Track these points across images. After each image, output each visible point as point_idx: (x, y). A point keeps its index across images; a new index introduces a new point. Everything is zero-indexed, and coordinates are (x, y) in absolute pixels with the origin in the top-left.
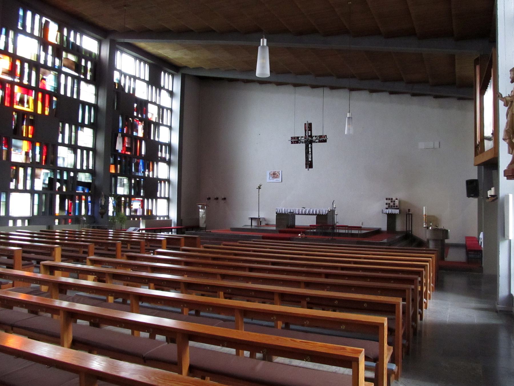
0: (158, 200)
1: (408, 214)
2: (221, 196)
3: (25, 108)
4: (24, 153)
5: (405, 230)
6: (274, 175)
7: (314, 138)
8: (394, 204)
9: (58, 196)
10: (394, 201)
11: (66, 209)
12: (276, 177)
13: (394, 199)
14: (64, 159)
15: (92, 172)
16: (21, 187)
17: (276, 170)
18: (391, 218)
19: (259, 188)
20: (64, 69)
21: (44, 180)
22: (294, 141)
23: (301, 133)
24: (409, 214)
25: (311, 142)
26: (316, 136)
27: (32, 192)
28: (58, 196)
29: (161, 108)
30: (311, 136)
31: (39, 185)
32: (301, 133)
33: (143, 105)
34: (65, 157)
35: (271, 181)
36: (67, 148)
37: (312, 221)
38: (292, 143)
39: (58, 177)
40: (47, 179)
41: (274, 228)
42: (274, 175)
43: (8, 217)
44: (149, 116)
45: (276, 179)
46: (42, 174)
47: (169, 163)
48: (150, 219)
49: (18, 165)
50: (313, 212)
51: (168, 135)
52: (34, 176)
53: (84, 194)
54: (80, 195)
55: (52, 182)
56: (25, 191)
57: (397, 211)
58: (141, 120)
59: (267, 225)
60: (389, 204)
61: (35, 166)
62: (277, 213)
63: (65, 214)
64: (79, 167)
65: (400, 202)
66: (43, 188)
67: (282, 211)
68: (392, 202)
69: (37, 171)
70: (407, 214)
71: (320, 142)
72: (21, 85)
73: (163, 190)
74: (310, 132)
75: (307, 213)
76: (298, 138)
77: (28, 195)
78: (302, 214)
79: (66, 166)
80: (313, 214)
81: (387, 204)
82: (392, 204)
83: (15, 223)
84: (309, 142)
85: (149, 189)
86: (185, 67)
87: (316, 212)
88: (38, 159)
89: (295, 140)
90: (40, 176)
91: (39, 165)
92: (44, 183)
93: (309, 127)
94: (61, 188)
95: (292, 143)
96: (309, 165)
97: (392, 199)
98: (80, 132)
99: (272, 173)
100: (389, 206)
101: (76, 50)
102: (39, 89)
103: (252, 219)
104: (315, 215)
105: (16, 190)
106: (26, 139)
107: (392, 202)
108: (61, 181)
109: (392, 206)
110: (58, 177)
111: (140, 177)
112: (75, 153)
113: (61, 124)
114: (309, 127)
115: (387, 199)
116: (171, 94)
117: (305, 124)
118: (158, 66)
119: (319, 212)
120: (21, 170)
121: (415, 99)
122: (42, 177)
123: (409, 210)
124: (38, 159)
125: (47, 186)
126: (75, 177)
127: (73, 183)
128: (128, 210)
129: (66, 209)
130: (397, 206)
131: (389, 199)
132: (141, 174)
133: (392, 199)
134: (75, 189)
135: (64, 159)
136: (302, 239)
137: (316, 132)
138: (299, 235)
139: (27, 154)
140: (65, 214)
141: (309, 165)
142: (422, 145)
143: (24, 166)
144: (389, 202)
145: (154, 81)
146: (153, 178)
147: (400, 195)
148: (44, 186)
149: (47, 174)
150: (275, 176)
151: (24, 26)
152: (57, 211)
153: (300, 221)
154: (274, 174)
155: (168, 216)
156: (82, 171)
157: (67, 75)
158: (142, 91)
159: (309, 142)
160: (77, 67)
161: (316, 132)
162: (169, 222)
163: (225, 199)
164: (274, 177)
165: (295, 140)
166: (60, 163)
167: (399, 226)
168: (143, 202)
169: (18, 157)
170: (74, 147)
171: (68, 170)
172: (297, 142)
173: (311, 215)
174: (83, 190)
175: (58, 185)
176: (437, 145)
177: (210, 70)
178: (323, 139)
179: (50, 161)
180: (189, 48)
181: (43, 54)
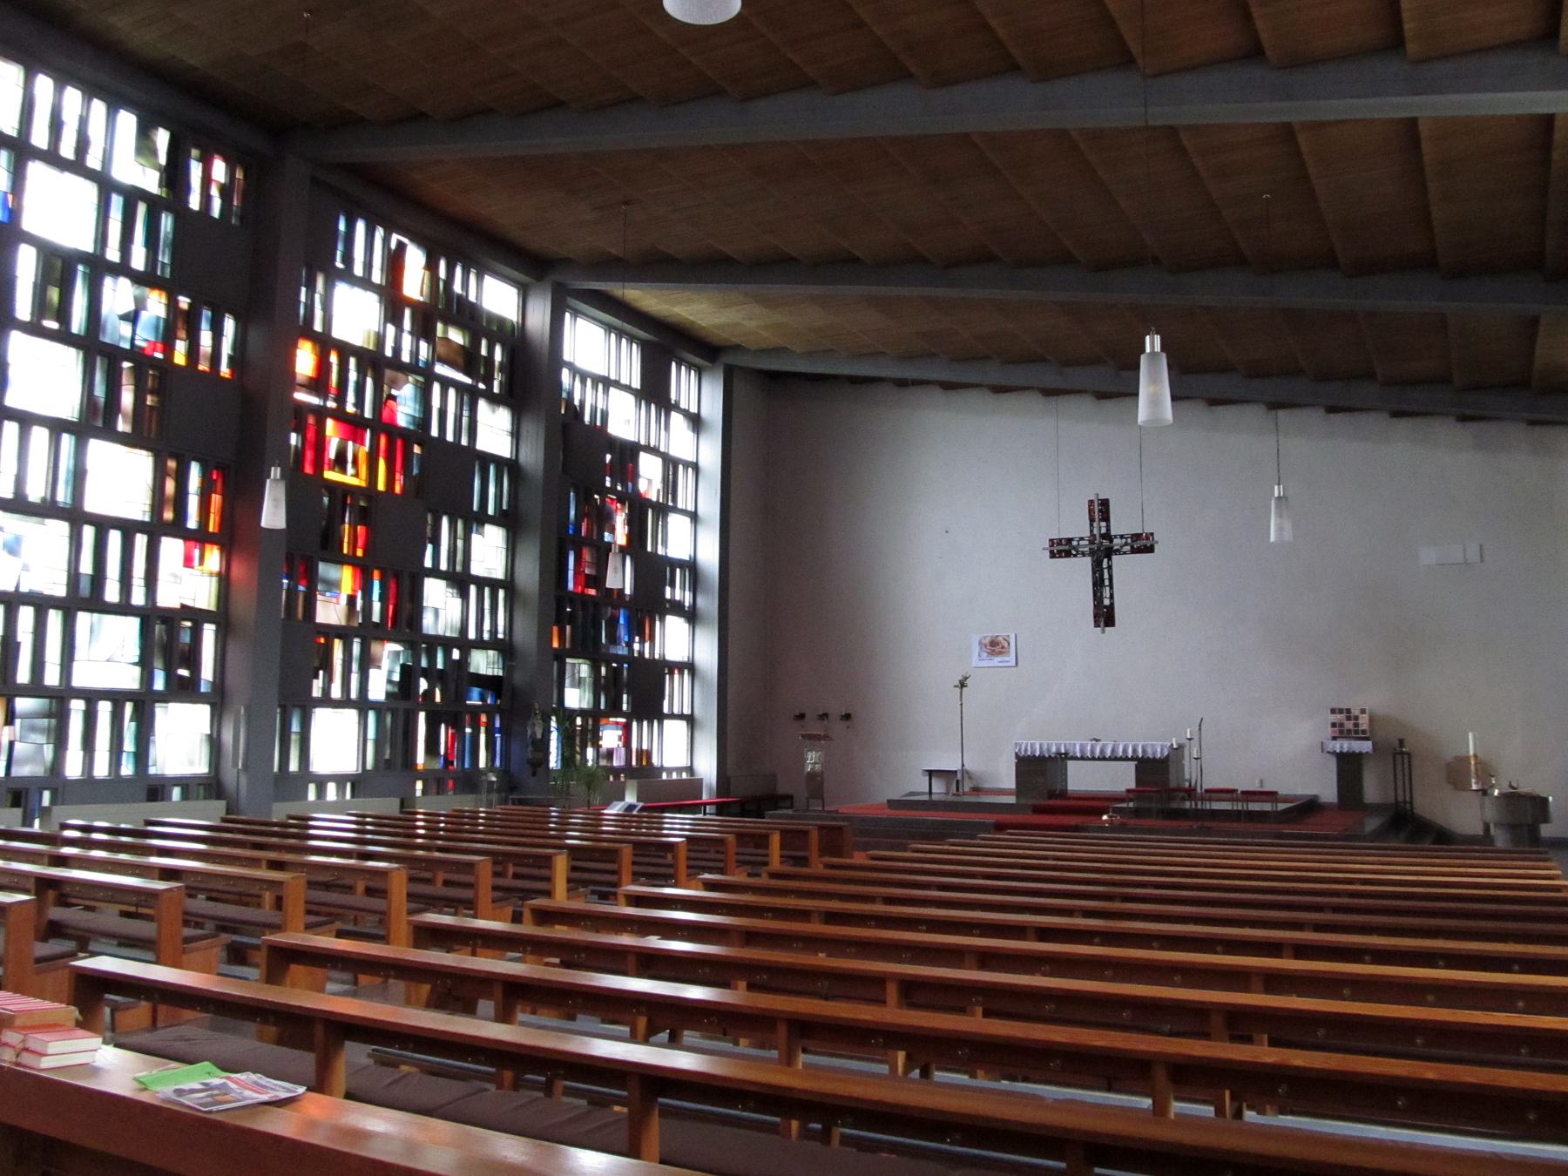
0: (666, 722)
1: (1399, 754)
2: (836, 709)
3: (348, 479)
4: (343, 600)
5: (1391, 800)
6: (995, 647)
7: (1116, 541)
8: (1356, 725)
9: (422, 716)
10: (1356, 718)
11: (442, 751)
12: (1000, 653)
13: (1355, 712)
14: (436, 611)
15: (505, 648)
16: (336, 693)
18: (1349, 766)
19: (962, 685)
20: (441, 369)
21: (390, 672)
22: (1060, 552)
23: (1078, 527)
24: (1402, 753)
25: (1110, 553)
26: (1122, 537)
27: (363, 705)
28: (422, 716)
29: (671, 464)
30: (1107, 536)
31: (378, 689)
32: (1078, 527)
33: (628, 453)
34: (441, 607)
35: (985, 664)
37: (1122, 779)
38: (1053, 555)
39: (424, 663)
40: (398, 669)
41: (1012, 800)
42: (995, 647)
43: (306, 775)
44: (642, 486)
45: (999, 658)
46: (385, 654)
47: (692, 616)
48: (647, 777)
49: (331, 632)
50: (1125, 751)
51: (692, 539)
52: (367, 662)
53: (485, 708)
54: (475, 712)
56: (345, 703)
57: (1366, 746)
58: (621, 500)
59: (976, 790)
60: (1342, 725)
62: (1017, 756)
64: (472, 635)
65: (1371, 720)
66: (388, 694)
68: (1348, 719)
69: (375, 647)
70: (1394, 755)
71: (1134, 551)
72: (340, 415)
73: (678, 693)
74: (1103, 524)
75: (1108, 753)
76: (1069, 540)
78: (1093, 759)
79: (441, 633)
80: (1126, 759)
81: (1334, 725)
82: (1349, 725)
83: (321, 792)
84: (1102, 552)
85: (639, 691)
86: (737, 348)
87: (1135, 751)
89: (1062, 549)
90: (380, 660)
92: (390, 681)
93: (1101, 510)
94: (429, 694)
95: (1053, 555)
96: (1105, 616)
97: (1349, 711)
98: (475, 537)
99: (987, 641)
100: (1341, 732)
101: (468, 315)
102: (382, 425)
103: (931, 773)
104: (1132, 759)
105: (326, 701)
106: (350, 560)
108: (429, 673)
109: (1349, 731)
110: (424, 663)
111: (620, 659)
113: (429, 517)
114: (1101, 510)
115: (1333, 711)
116: (696, 422)
117: (1091, 502)
118: (665, 346)
119: (1144, 751)
120: (338, 646)
121: (1403, 424)
122: (386, 663)
123: (1401, 742)
124: (376, 618)
126: (464, 661)
127: (458, 678)
128: (590, 752)
129: (442, 751)
130: (1364, 732)
131: (1341, 711)
132: (622, 650)
133: (1349, 711)
134: (462, 696)
135: (436, 611)
136: (1113, 828)
137: (1122, 524)
138: (1105, 817)
139: (351, 600)
140: (438, 764)
141: (1105, 616)
142: (1428, 556)
143: (345, 633)
145: (654, 392)
146: (652, 661)
147: (1372, 698)
148: (390, 688)
149: (397, 654)
150: (997, 649)
151: (348, 259)
152: (421, 758)
153: (1081, 779)
154: (994, 643)
155: (690, 769)
156: (480, 644)
157: (446, 383)
158: (624, 418)
159: (1102, 552)
160: (468, 360)
161: (1122, 524)
162: (695, 785)
163: (847, 717)
164: (992, 653)
165: (1062, 549)
166: (429, 624)
167: (1373, 789)
168: (627, 729)
169: (330, 612)
170: (460, 580)
171: (447, 643)
172: (1068, 554)
173: (1121, 759)
174: (483, 698)
175: (423, 685)
176: (1473, 555)
177: (809, 354)
178: (1142, 545)
179: (404, 619)
180: (769, 303)
181: (391, 330)
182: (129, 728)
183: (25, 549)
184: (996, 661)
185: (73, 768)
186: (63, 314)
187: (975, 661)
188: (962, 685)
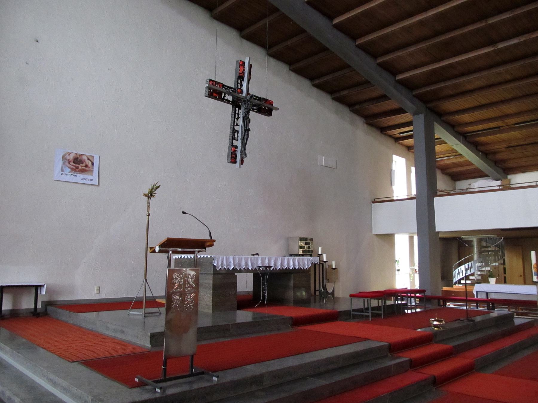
6: (79, 164)
8: (309, 248)
12: (83, 171)
17: (84, 151)
19: (151, 194)
22: (215, 91)
45: (82, 176)
67: (228, 264)
81: (301, 247)
89: (216, 91)
99: (71, 157)
107: (306, 244)
115: (301, 239)
121: (315, 90)
130: (312, 251)
144: (302, 244)
150: (81, 167)
154: (77, 160)
164: (76, 170)
178: (265, 108)
184: (79, 177)
187: (57, 173)
188: (151, 194)
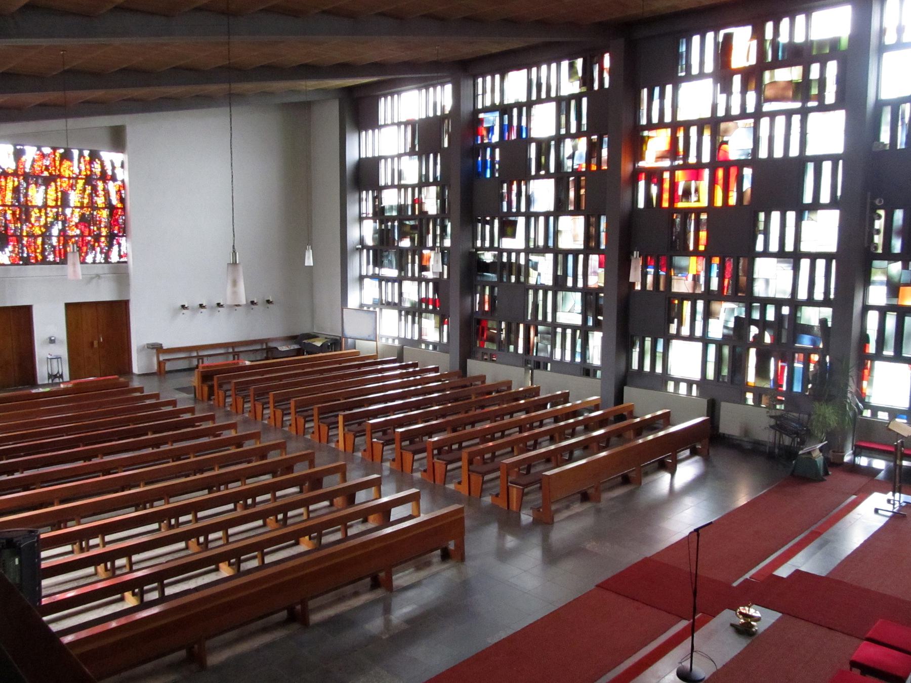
3: (692, 204)
4: (690, 278)
9: (753, 352)
14: (767, 281)
16: (685, 331)
21: (726, 321)
27: (705, 341)
28: (753, 352)
31: (716, 330)
34: (771, 278)
36: (775, 260)
39: (756, 315)
40: (733, 320)
43: (665, 377)
46: (722, 310)
49: (683, 297)
52: (708, 314)
55: (741, 325)
56: (691, 338)
61: (709, 297)
63: (768, 385)
64: (802, 295)
66: (724, 336)
69: (715, 306)
72: (685, 167)
77: (699, 345)
83: (677, 386)
88: (714, 286)
90: (719, 314)
91: (720, 296)
92: (725, 327)
94: (759, 337)
101: (798, 55)
102: (719, 162)
105: (678, 336)
106: (696, 253)
110: (756, 315)
112: (796, 269)
120: (687, 305)
122: (723, 316)
124: (714, 286)
125: (731, 333)
135: (767, 281)
139: (696, 278)
143: (693, 298)
148: (726, 331)
149: (733, 310)
151: (688, 67)
152: (751, 377)
156: (811, 302)
166: (759, 290)
169: (682, 285)
171: (778, 303)
175: (754, 330)
181: (722, 99)
182: (579, 342)
183: (539, 266)
185: (558, 356)
186: (547, 168)
